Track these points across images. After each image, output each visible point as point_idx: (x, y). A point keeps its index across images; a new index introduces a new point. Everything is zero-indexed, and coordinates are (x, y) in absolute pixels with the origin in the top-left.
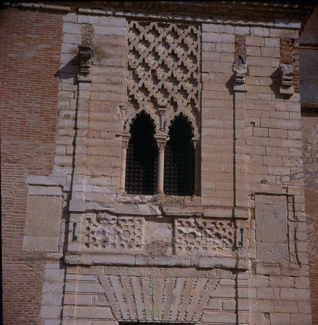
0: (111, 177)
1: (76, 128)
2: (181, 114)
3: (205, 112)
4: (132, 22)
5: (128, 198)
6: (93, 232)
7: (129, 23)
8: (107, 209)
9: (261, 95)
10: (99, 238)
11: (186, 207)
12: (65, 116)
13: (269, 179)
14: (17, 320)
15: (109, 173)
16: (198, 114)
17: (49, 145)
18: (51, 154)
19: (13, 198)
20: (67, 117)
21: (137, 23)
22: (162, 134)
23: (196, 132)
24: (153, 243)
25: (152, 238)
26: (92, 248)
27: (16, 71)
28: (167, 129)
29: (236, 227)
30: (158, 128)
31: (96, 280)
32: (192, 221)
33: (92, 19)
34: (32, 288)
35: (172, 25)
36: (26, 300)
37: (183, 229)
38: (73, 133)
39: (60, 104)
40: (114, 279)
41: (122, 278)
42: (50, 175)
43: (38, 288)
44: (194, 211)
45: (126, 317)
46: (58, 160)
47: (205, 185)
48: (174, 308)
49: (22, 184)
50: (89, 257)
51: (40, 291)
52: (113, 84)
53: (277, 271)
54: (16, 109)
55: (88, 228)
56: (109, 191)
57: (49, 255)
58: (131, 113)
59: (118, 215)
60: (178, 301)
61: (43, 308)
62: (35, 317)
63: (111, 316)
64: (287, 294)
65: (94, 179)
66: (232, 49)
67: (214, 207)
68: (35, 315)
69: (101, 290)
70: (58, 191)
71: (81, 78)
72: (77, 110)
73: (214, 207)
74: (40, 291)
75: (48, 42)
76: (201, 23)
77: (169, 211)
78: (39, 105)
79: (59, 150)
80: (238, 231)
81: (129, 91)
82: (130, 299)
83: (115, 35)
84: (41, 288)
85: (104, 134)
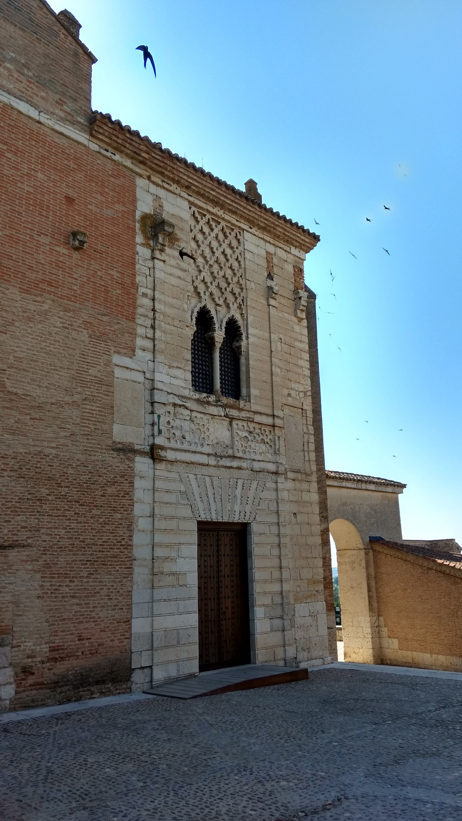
0: (185, 370)
1: (154, 310)
2: (233, 316)
3: (250, 319)
4: (193, 208)
6: (172, 427)
7: (190, 208)
8: (184, 404)
9: (285, 314)
10: (178, 433)
12: (143, 293)
13: (293, 393)
14: (114, 517)
15: (182, 366)
16: (245, 319)
18: (134, 335)
19: (102, 377)
20: (145, 295)
21: (196, 210)
24: (217, 443)
25: (217, 438)
26: (173, 444)
27: (97, 227)
28: (224, 330)
29: (275, 435)
30: (217, 326)
31: (178, 477)
33: (161, 193)
34: (125, 482)
35: (223, 223)
36: (121, 496)
37: (240, 433)
38: (151, 314)
40: (192, 477)
41: (199, 476)
42: (134, 357)
43: (130, 483)
44: (248, 416)
46: (140, 342)
47: (254, 392)
48: (237, 508)
49: (108, 363)
51: (131, 486)
52: (182, 270)
53: (299, 476)
55: (169, 423)
56: (184, 385)
57: (136, 447)
59: (191, 411)
60: (239, 501)
61: (136, 505)
62: (129, 514)
63: (192, 516)
64: (306, 497)
65: (171, 369)
67: (260, 413)
68: (129, 512)
69: (183, 489)
70: (140, 377)
72: (154, 290)
73: (260, 413)
74: (131, 486)
75: (124, 205)
76: (243, 230)
77: (230, 413)
78: (119, 275)
79: (140, 331)
80: (277, 438)
81: (193, 281)
82: (205, 499)
83: (180, 218)
84: (133, 483)
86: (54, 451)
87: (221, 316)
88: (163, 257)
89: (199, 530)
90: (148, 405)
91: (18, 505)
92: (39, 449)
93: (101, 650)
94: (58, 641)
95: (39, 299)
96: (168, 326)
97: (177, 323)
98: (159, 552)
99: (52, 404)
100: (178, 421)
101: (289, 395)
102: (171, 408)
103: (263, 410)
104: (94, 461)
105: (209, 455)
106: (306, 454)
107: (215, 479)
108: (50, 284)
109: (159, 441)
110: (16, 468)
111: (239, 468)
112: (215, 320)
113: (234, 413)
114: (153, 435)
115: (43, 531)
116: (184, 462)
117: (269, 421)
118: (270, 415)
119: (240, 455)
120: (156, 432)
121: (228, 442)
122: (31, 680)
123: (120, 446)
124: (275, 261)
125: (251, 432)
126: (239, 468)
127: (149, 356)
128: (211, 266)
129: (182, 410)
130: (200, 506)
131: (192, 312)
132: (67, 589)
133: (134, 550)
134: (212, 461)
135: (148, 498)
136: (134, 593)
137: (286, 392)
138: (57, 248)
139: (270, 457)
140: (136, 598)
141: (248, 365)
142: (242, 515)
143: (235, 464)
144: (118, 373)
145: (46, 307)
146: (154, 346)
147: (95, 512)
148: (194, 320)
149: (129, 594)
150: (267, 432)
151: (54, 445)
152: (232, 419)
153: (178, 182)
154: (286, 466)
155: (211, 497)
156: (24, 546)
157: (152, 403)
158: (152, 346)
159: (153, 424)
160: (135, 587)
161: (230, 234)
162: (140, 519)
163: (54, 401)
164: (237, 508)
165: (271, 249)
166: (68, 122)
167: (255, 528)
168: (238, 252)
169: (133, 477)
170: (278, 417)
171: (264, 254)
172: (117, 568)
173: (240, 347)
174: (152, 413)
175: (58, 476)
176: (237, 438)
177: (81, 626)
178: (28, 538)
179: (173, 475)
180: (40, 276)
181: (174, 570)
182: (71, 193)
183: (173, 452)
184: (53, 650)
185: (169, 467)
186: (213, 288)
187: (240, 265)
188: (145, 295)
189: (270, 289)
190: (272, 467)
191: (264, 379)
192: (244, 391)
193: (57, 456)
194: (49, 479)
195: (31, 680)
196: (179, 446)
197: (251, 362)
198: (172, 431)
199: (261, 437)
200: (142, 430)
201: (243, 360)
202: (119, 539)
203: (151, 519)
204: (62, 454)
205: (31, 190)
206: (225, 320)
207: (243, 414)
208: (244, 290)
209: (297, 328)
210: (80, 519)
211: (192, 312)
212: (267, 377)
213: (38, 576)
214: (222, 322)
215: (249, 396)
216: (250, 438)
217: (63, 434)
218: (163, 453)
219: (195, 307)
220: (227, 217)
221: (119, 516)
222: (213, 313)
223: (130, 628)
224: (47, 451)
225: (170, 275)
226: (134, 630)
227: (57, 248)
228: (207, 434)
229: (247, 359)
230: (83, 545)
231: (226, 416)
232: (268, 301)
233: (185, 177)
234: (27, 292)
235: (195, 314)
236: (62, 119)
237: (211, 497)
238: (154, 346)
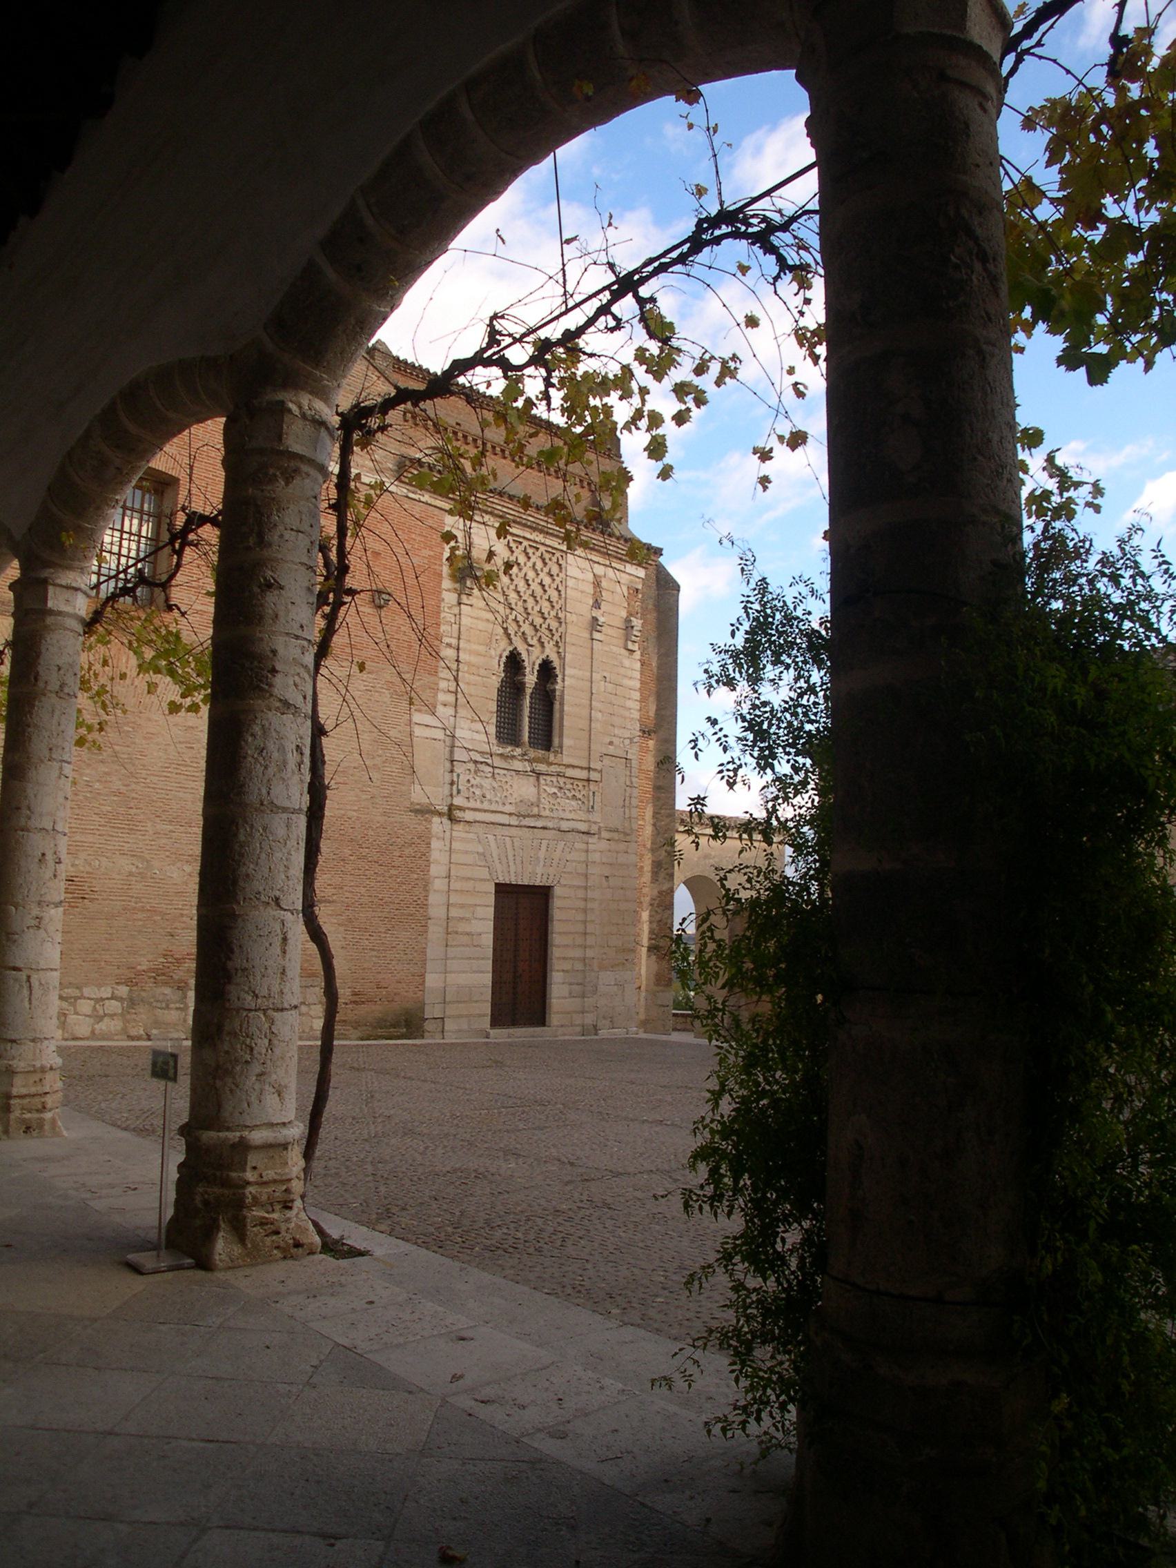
3: (568, 657)
5: (501, 751)
10: (478, 792)
11: (552, 764)
13: (616, 740)
17: (432, 679)
18: (435, 690)
20: (449, 645)
22: (531, 679)
23: (559, 680)
26: (472, 804)
28: (536, 673)
30: (528, 670)
32: (554, 779)
38: (454, 666)
39: (443, 628)
40: (491, 837)
41: (499, 837)
45: (501, 878)
46: (442, 697)
48: (539, 870)
50: (472, 813)
53: (616, 836)
54: (403, 628)
55: (468, 781)
58: (504, 649)
60: (542, 863)
61: (432, 865)
66: (590, 589)
67: (573, 767)
69: (481, 850)
70: (439, 734)
71: (464, 598)
72: (459, 639)
73: (573, 767)
79: (443, 685)
80: (591, 794)
85: (482, 672)
86: (355, 814)
87: (533, 658)
88: (472, 600)
89: (496, 892)
90: (448, 765)
92: (343, 812)
93: (397, 998)
94: (358, 988)
96: (472, 677)
97: (482, 672)
98: (454, 913)
100: (478, 779)
101: (611, 743)
102: (471, 766)
103: (575, 763)
104: (391, 823)
105: (510, 814)
106: (627, 811)
107: (515, 840)
109: (458, 801)
111: (544, 828)
112: (526, 664)
113: (542, 767)
114: (451, 795)
115: (345, 888)
116: (483, 822)
117: (583, 774)
118: (585, 768)
119: (547, 813)
120: (455, 792)
121: (534, 800)
123: (418, 807)
124: (604, 584)
125: (561, 788)
126: (544, 828)
127: (451, 711)
128: (525, 601)
129: (482, 767)
130: (499, 867)
131: (501, 657)
132: (367, 942)
133: (430, 910)
134: (514, 821)
135: (444, 859)
136: (428, 950)
137: (608, 740)
139: (583, 816)
140: (430, 954)
141: (562, 711)
142: (545, 877)
143: (539, 824)
144: (418, 731)
146: (457, 699)
147: (393, 872)
148: (502, 665)
149: (424, 952)
150: (581, 788)
152: (538, 775)
153: (491, 513)
154: (601, 825)
155: (511, 858)
156: (329, 902)
157: (452, 761)
158: (454, 699)
159: (452, 783)
160: (429, 944)
161: (550, 559)
162: (436, 880)
163: (356, 765)
164: (539, 870)
165: (599, 570)
167: (558, 891)
168: (558, 580)
169: (430, 838)
170: (595, 770)
171: (590, 577)
172: (413, 926)
173: (554, 690)
174: (452, 771)
176: (544, 795)
177: (380, 976)
179: (471, 836)
181: (468, 930)
183: (472, 812)
184: (355, 994)
185: (467, 828)
186: (526, 628)
187: (560, 595)
188: (449, 645)
189: (595, 619)
190: (583, 827)
191: (580, 726)
192: (556, 741)
193: (358, 818)
196: (478, 805)
197: (566, 708)
198: (472, 790)
199: (573, 793)
200: (440, 789)
201: (557, 706)
202: (415, 898)
203: (447, 880)
204: (363, 816)
206: (539, 661)
207: (553, 769)
208: (563, 624)
209: (627, 663)
210: (379, 879)
211: (501, 657)
212: (584, 724)
213: (342, 929)
214: (534, 664)
215: (561, 746)
216: (559, 794)
217: (364, 797)
218: (458, 814)
219: (504, 650)
220: (548, 542)
221: (416, 876)
222: (524, 656)
223: (424, 981)
224: (351, 814)
225: (477, 618)
226: (427, 984)
228: (510, 791)
229: (562, 704)
230: (381, 902)
231: (533, 771)
232: (591, 634)
233: (499, 508)
235: (504, 659)
237: (511, 858)
238: (457, 699)
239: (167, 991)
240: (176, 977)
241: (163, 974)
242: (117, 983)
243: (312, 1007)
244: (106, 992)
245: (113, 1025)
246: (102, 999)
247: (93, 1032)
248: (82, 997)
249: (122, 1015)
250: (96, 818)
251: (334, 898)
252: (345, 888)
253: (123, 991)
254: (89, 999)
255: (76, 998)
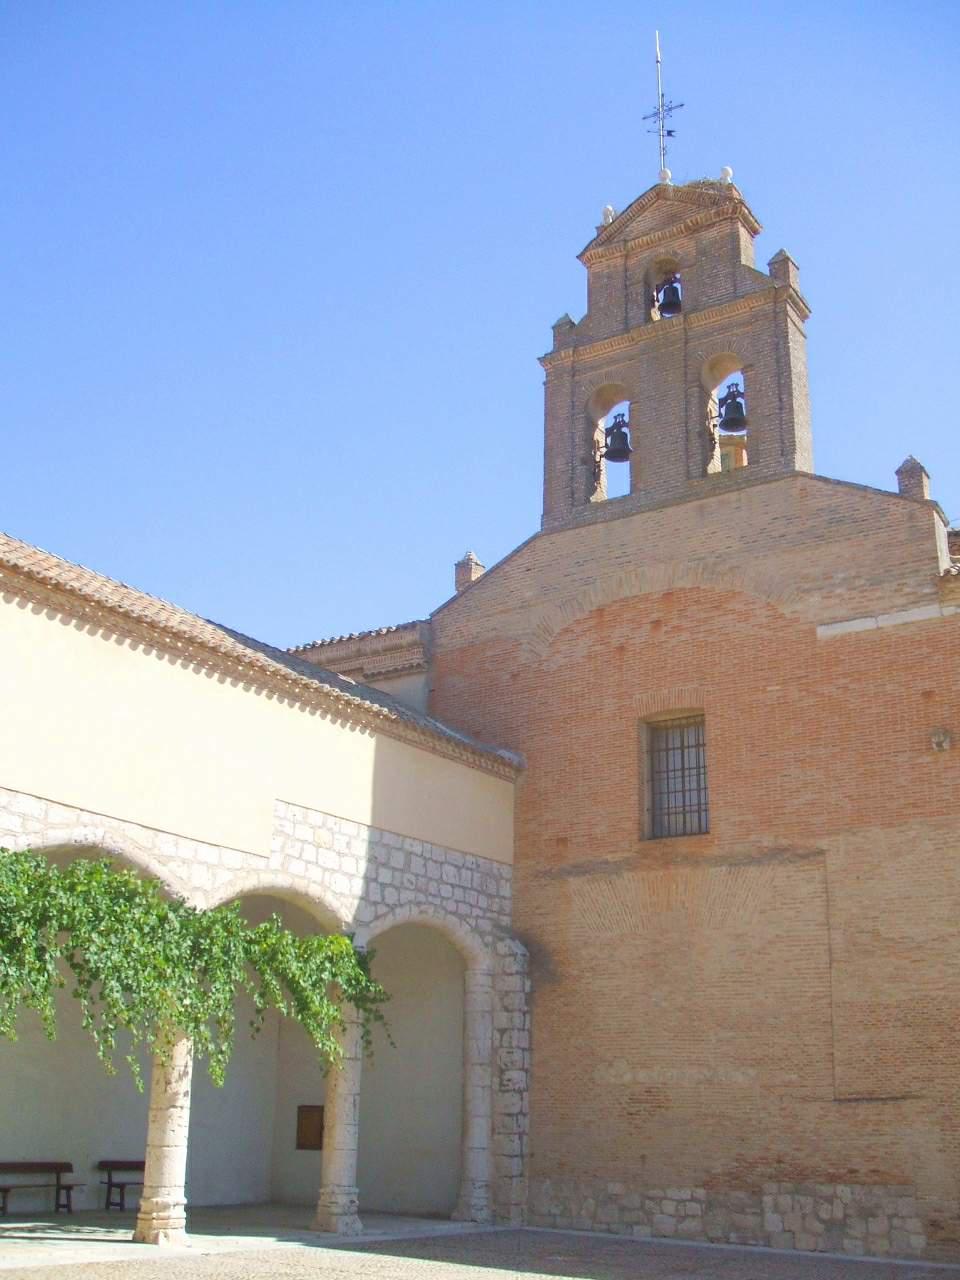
86: (943, 993)
91: (907, 1055)
92: (923, 993)
95: (903, 828)
99: (934, 940)
108: (915, 805)
110: (900, 1017)
122: (942, 1234)
138: (920, 761)
145: (912, 833)
151: (941, 985)
166: (911, 606)
175: (949, 1019)
178: (922, 1089)
180: (902, 801)
182: (927, 685)
194: (939, 1024)
195: (942, 1234)
205: (882, 710)
217: (951, 971)
224: (933, 994)
227: (920, 761)
234: (891, 825)
236: (904, 608)
239: (741, 1194)
240: (749, 1180)
241: (737, 1178)
242: (696, 1186)
243: (908, 1220)
244: (686, 1194)
245: (691, 1225)
246: (684, 1201)
247: (676, 1231)
248: (665, 1198)
249: (702, 1217)
250: (666, 1033)
251: (924, 1092)
252: (937, 1081)
253: (701, 1193)
254: (673, 1200)
255: (662, 1199)
